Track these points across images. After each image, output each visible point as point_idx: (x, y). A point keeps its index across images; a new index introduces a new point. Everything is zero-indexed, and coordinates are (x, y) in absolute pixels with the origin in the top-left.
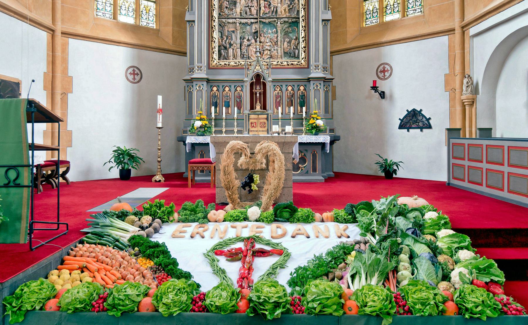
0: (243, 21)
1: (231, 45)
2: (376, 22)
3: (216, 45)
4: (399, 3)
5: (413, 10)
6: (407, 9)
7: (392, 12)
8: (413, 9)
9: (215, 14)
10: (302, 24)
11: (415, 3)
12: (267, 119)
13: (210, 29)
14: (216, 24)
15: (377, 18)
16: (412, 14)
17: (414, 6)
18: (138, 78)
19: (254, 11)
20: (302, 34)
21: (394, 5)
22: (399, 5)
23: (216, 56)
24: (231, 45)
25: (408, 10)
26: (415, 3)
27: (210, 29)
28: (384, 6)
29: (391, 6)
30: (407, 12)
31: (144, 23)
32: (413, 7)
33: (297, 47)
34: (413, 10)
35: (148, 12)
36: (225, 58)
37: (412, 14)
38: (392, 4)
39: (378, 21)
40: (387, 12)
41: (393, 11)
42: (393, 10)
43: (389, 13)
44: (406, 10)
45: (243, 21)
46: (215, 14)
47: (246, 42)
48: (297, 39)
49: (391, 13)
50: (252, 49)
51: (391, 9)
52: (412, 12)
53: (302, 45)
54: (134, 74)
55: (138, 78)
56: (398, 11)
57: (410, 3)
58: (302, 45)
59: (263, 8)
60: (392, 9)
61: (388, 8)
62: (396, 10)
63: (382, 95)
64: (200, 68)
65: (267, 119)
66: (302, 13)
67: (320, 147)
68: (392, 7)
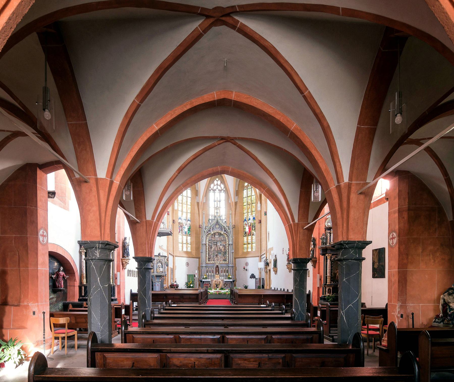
0: (214, 252)
1: (211, 258)
3: (207, 258)
9: (207, 250)
10: (227, 253)
12: (219, 276)
13: (206, 254)
14: (207, 253)
18: (188, 265)
19: (216, 250)
20: (227, 255)
23: (207, 261)
24: (211, 258)
27: (206, 254)
31: (188, 251)
33: (226, 259)
35: (189, 247)
36: (210, 261)
45: (214, 252)
46: (207, 250)
47: (214, 257)
48: (226, 256)
50: (216, 259)
53: (227, 258)
54: (187, 264)
55: (188, 265)
58: (227, 258)
59: (218, 249)
63: (246, 270)
64: (204, 264)
65: (219, 276)
66: (227, 251)
67: (230, 282)
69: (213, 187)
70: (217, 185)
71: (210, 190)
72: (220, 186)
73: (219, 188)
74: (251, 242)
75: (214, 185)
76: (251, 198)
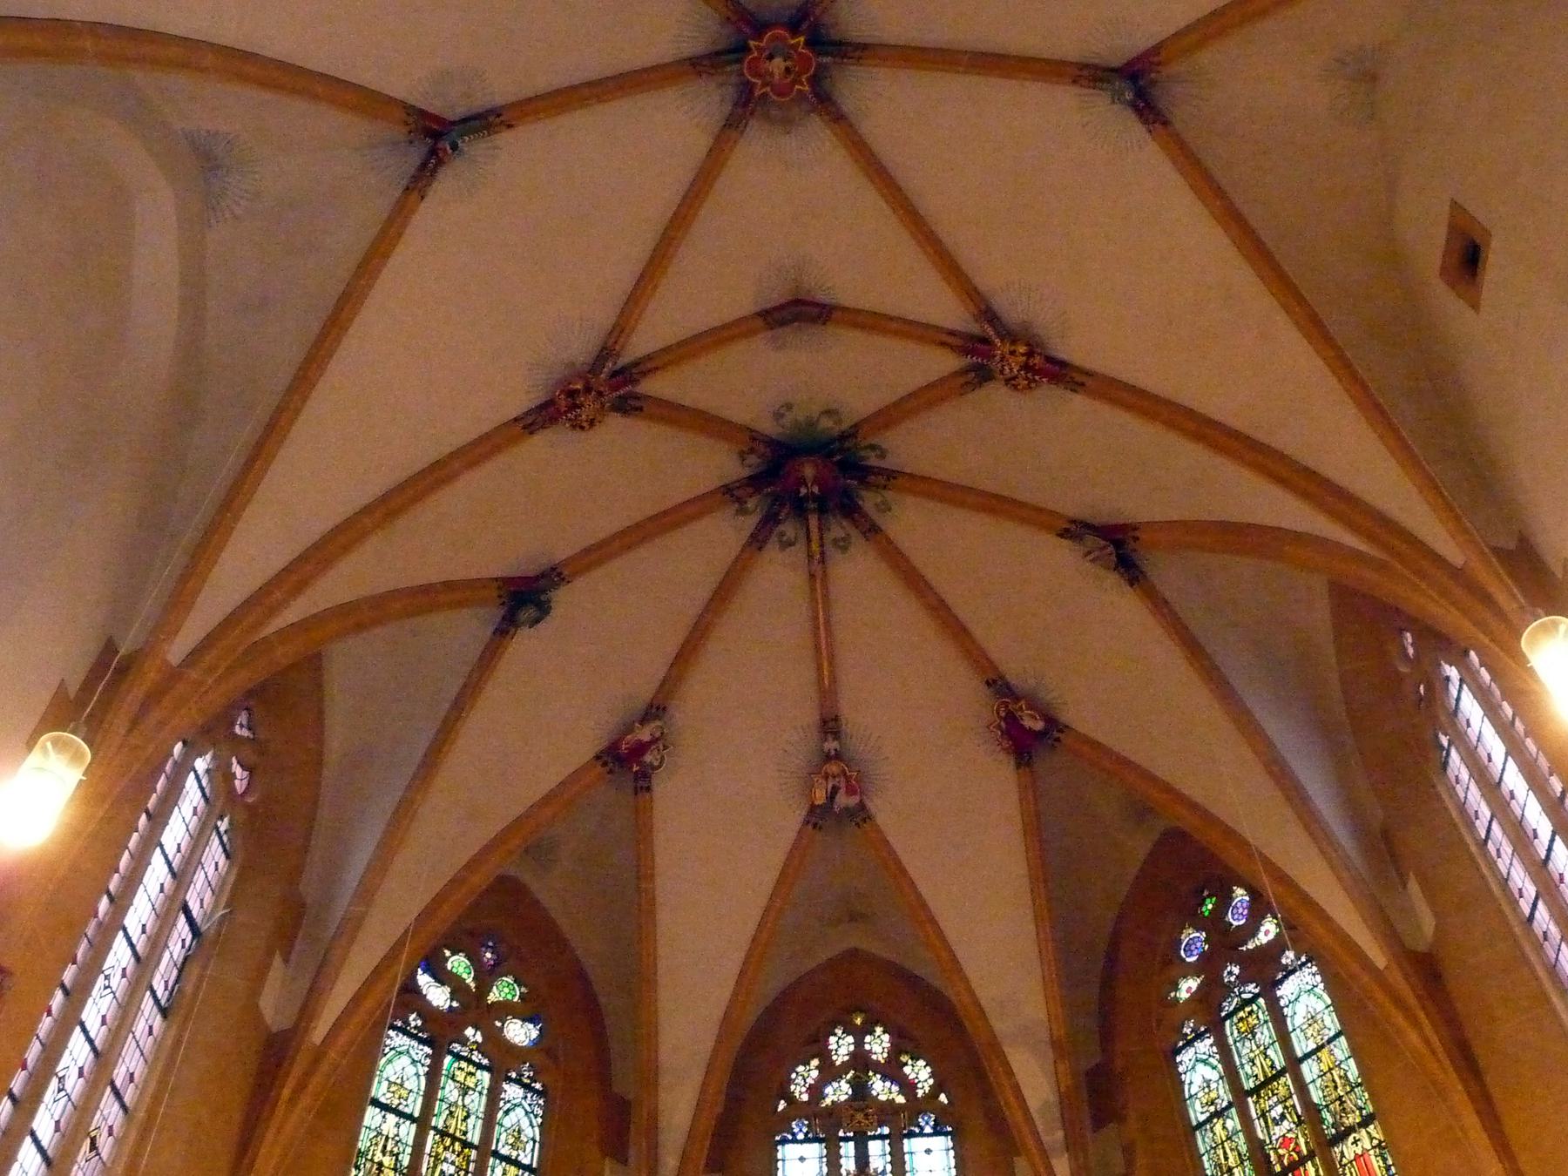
69: (816, 1091)
70: (861, 1062)
71: (784, 1122)
72: (892, 1071)
73: (880, 1088)
75: (830, 1072)
76: (1302, 1088)
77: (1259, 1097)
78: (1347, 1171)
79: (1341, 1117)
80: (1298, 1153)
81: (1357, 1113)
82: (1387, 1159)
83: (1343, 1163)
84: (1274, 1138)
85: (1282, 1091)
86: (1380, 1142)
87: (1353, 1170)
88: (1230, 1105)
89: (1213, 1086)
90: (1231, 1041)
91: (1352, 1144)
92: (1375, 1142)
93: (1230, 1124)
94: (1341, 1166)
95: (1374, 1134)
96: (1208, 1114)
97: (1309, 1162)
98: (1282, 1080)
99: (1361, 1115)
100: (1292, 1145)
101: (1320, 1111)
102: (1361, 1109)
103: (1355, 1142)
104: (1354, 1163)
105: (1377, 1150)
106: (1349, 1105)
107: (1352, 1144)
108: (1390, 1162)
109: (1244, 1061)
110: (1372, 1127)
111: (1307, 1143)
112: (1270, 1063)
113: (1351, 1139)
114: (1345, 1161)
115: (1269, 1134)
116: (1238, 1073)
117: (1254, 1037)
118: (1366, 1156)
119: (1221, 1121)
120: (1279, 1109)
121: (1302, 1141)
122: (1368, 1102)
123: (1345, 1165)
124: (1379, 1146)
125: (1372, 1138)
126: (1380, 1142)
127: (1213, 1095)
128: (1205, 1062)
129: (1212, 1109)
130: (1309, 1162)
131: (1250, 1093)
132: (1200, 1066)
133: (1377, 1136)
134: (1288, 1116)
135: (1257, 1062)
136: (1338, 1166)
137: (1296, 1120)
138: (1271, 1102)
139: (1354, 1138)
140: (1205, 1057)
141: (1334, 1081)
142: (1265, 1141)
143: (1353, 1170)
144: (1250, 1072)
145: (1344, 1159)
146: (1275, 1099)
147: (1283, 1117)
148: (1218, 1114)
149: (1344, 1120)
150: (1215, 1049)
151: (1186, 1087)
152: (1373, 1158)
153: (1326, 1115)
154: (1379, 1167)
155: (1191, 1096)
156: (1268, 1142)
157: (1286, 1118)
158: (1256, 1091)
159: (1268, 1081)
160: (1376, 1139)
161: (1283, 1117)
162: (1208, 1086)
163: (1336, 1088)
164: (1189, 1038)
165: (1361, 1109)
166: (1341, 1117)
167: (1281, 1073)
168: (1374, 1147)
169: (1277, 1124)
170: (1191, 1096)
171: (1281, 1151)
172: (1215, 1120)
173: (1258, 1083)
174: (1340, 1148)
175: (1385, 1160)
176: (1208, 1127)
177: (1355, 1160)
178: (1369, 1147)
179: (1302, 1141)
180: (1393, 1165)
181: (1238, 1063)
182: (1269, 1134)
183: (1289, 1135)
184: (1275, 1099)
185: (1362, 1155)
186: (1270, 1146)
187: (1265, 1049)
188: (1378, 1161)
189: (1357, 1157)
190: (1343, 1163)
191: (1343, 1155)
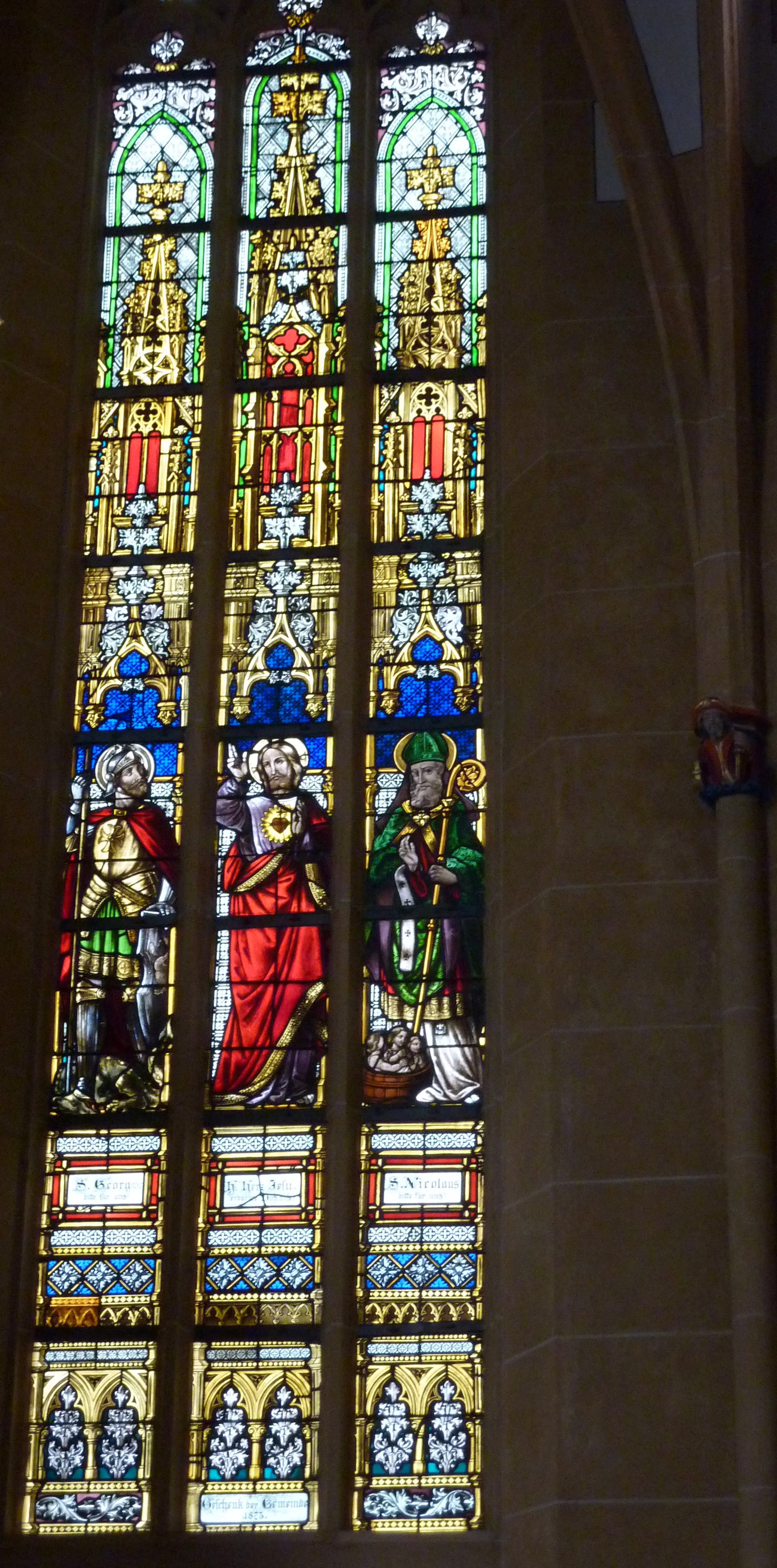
2: (121, 1517)
4: (309, 1420)
5: (410, 1492)
6: (368, 1478)
7: (254, 1472)
8: (411, 1482)
11: (426, 1449)
15: (132, 1486)
16: (400, 1515)
17: (418, 1467)
21: (266, 1420)
22: (306, 1432)
25: (377, 1482)
26: (426, 1449)
28: (195, 1415)
29: (245, 1420)
30: (365, 1491)
32: (405, 1469)
34: (410, 1492)
37: (400, 1515)
38: (256, 1413)
39: (138, 1513)
40: (215, 1460)
41: (263, 1464)
42: (264, 1457)
43: (229, 1470)
44: (359, 1482)
49: (241, 1474)
51: (244, 1443)
52: (402, 1502)
56: (296, 1473)
57: (386, 1435)
60: (256, 1448)
61: (229, 1431)
62: (286, 1461)
68: (256, 1431)
74: (296, 1273)
77: (267, 238)
78: (390, 435)
79: (418, 345)
80: (306, 365)
81: (453, 352)
82: (475, 449)
83: (388, 419)
84: (268, 320)
85: (319, 252)
86: (475, 417)
87: (402, 438)
88: (200, 226)
89: (178, 176)
90: (248, 116)
91: (420, 397)
92: (465, 414)
93: (186, 257)
94: (383, 421)
95: (469, 400)
96: (146, 220)
97: (322, 391)
98: (328, 233)
99: (459, 360)
100: (300, 348)
101: (381, 318)
102: (462, 350)
103: (428, 397)
104: (410, 427)
105: (464, 427)
106: (442, 333)
107: (420, 397)
108: (480, 455)
109: (261, 165)
110: (471, 387)
111: (331, 357)
112: (314, 193)
113: (422, 388)
114: (393, 417)
115: (261, 307)
116: (241, 180)
117: (301, 133)
118: (438, 427)
119: (169, 244)
120: (301, 278)
121: (323, 349)
122: (482, 346)
123: (391, 425)
124: (471, 421)
125: (461, 406)
126: (475, 417)
127: (171, 192)
128: (177, 127)
129: (160, 215)
130: (322, 391)
131: (254, 224)
132: (163, 132)
133: (474, 406)
134: (313, 296)
135: (289, 179)
136: (377, 421)
137: (326, 310)
138: (287, 258)
139: (429, 390)
140: (181, 119)
141: (430, 280)
142: (248, 318)
143: (402, 438)
144: (266, 188)
145: (393, 414)
146: (299, 257)
147: (302, 294)
148: (169, 230)
149: (423, 354)
150: (210, 114)
151: (119, 153)
152: (449, 436)
153: (388, 326)
154: (455, 455)
155: (122, 173)
156: (253, 320)
157: (308, 298)
158: (266, 226)
159: (296, 221)
160: (469, 409)
161: (302, 294)
162: (168, 173)
163: (430, 294)
164: (160, 68)
165: (462, 350)
166: (418, 345)
167: (333, 220)
168: (457, 420)
169: (284, 301)
170: (122, 173)
171: (273, 348)
172: (158, 237)
173: (275, 214)
174: (393, 395)
175: (470, 448)
176: (138, 241)
177: (413, 423)
178: (450, 416)
179: (323, 349)
180: (482, 462)
181: (247, 161)
182: (261, 307)
183: (302, 330)
184: (299, 257)
185: (431, 423)
186: (254, 330)
187: (317, 165)
188: (456, 445)
189: (420, 421)
190: (388, 419)
191: (394, 406)
